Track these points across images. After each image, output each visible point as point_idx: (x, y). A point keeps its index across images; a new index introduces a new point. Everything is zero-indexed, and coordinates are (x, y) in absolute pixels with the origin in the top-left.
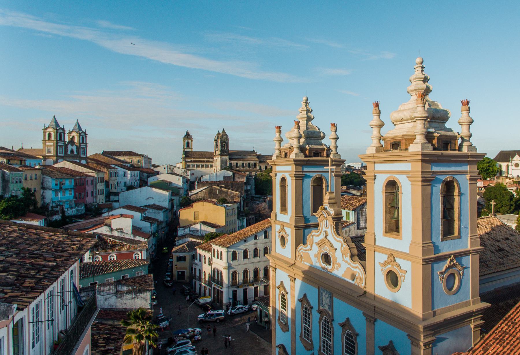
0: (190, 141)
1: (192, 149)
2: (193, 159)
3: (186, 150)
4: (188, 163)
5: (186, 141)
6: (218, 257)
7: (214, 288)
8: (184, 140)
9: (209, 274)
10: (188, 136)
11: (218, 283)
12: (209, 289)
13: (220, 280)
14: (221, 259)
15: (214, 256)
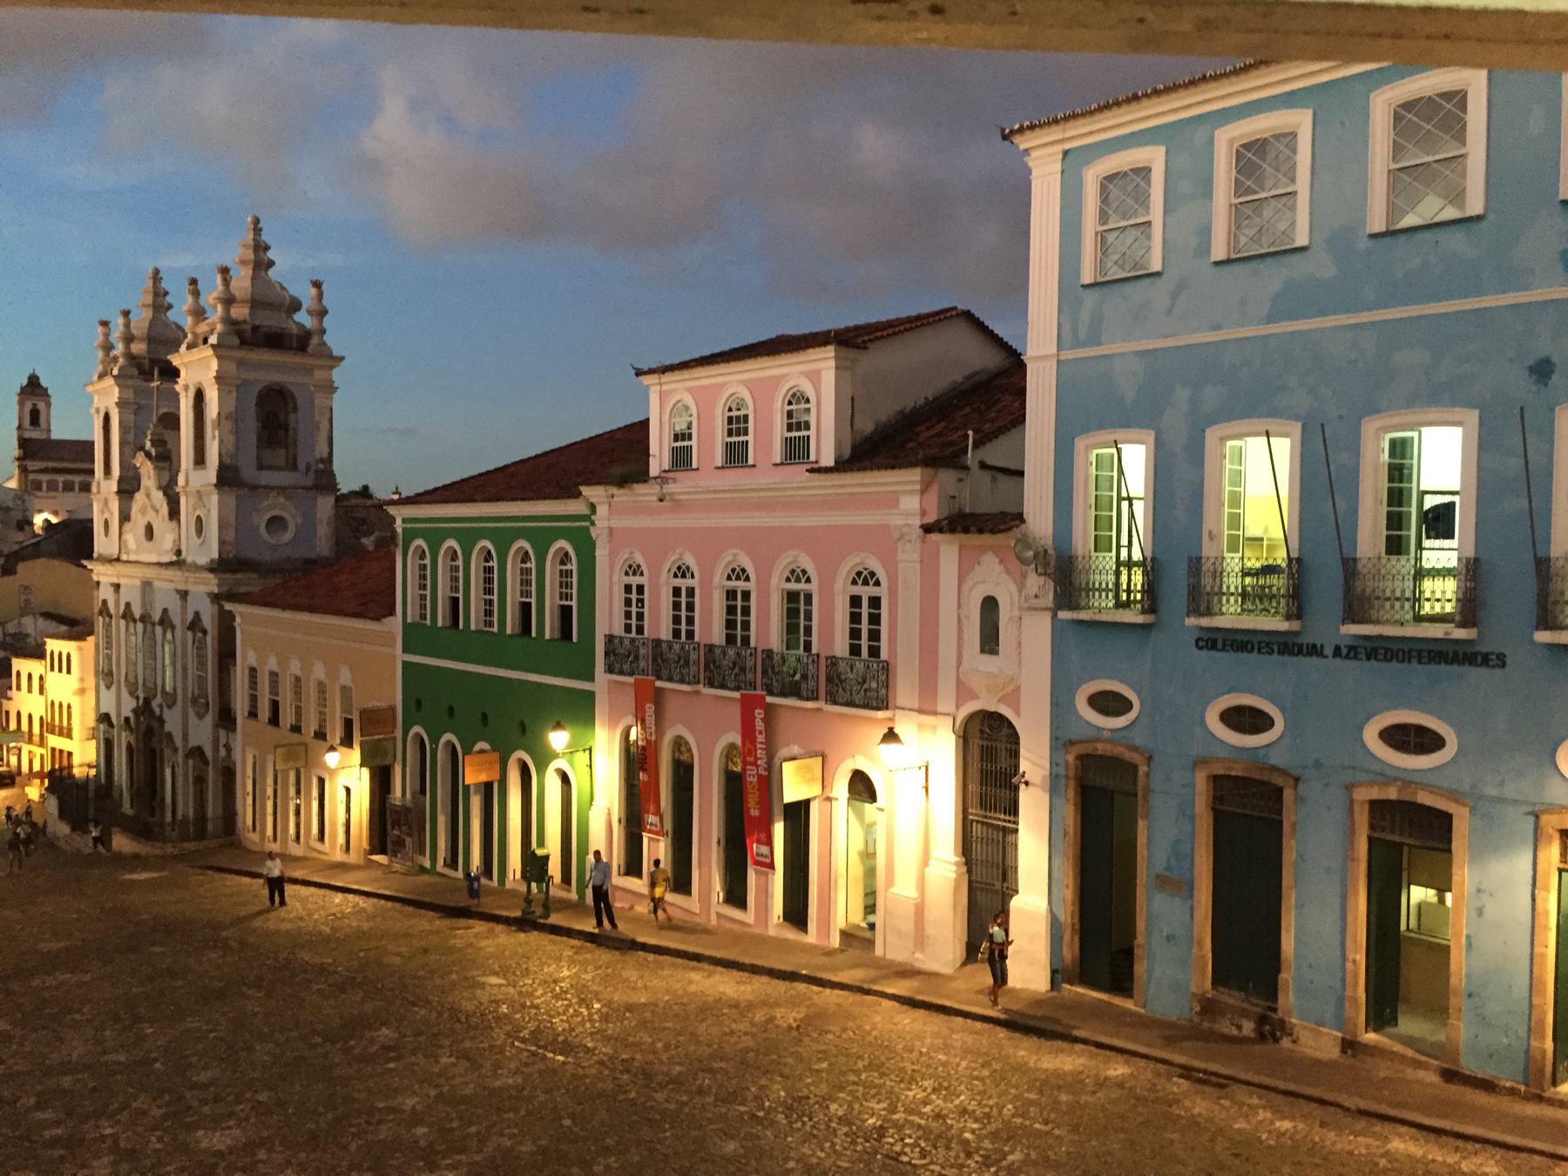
0: (41, 406)
1: (49, 431)
2: (51, 464)
3: (27, 435)
4: (31, 477)
5: (28, 406)
6: (60, 670)
7: (53, 750)
8: (21, 403)
9: (41, 718)
10: (33, 388)
11: (61, 734)
12: (42, 756)
13: (65, 723)
14: (69, 672)
15: (52, 669)
